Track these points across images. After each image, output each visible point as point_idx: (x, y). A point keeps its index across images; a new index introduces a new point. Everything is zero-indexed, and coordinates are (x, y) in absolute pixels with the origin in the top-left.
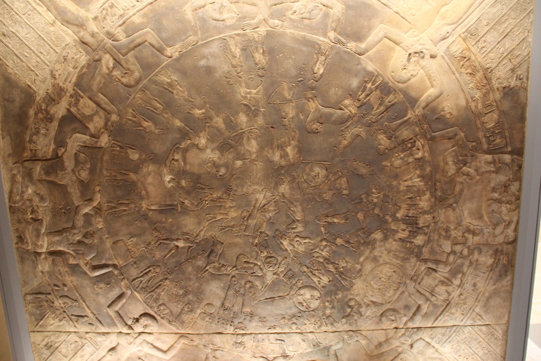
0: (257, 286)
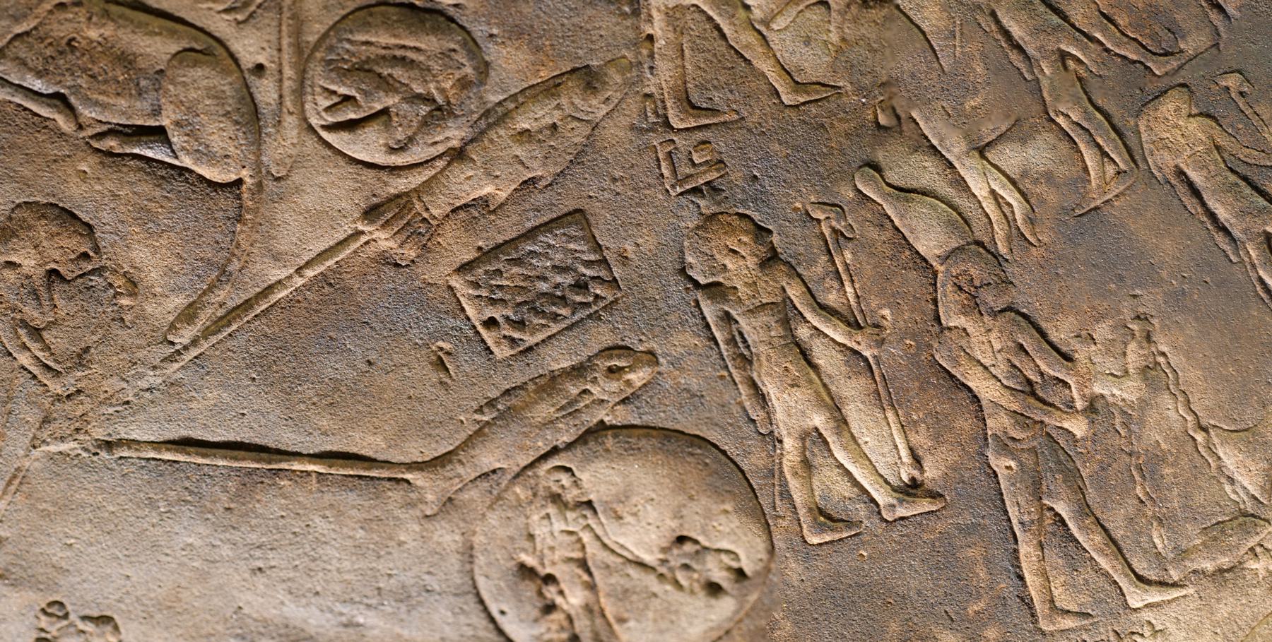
0: (133, 285)
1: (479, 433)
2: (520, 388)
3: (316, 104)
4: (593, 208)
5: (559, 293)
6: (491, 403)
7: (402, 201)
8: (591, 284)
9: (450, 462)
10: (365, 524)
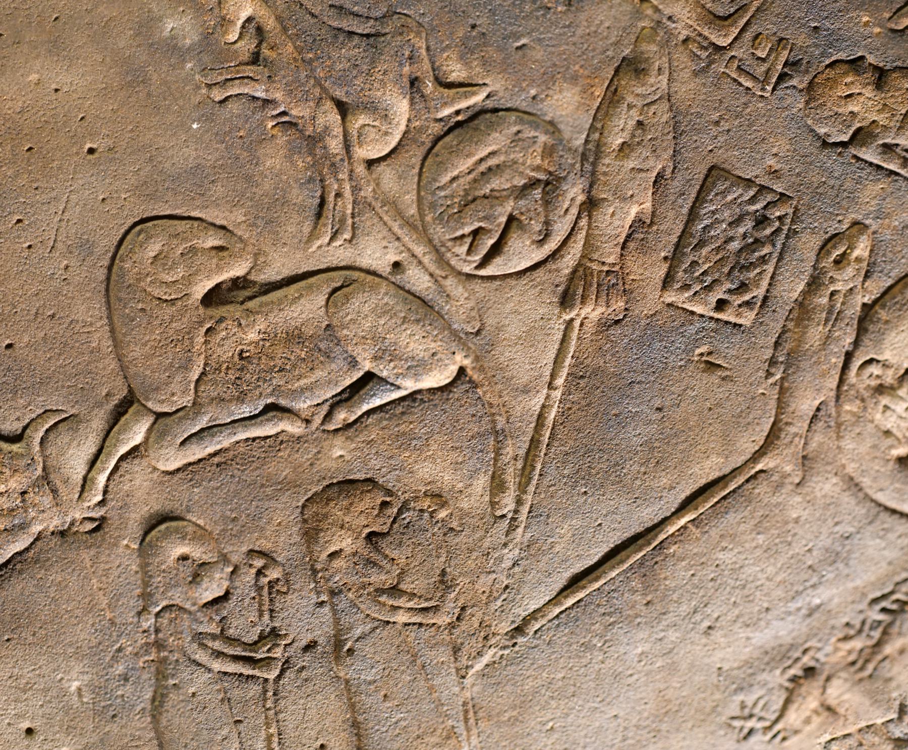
0: (437, 497)
1: (782, 391)
2: (783, 332)
3: (457, 256)
4: (721, 156)
5: (751, 240)
6: (772, 362)
7: (580, 273)
8: (768, 213)
9: (780, 430)
10: (758, 529)
